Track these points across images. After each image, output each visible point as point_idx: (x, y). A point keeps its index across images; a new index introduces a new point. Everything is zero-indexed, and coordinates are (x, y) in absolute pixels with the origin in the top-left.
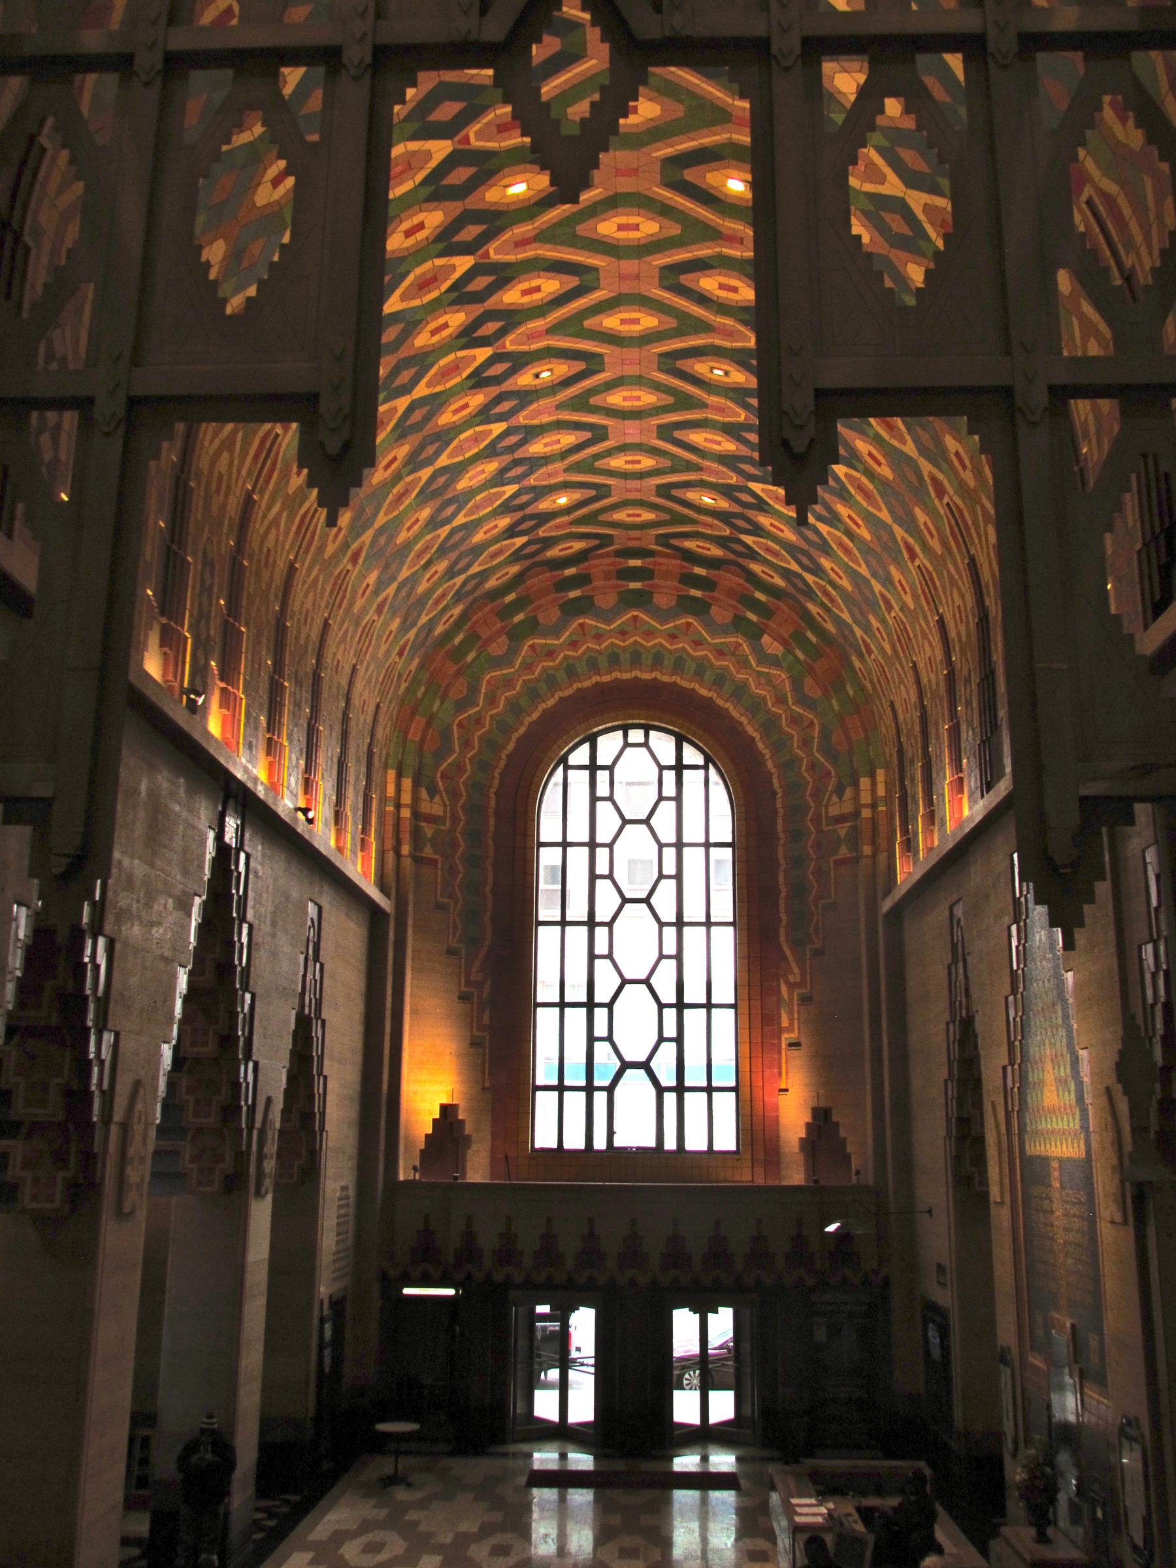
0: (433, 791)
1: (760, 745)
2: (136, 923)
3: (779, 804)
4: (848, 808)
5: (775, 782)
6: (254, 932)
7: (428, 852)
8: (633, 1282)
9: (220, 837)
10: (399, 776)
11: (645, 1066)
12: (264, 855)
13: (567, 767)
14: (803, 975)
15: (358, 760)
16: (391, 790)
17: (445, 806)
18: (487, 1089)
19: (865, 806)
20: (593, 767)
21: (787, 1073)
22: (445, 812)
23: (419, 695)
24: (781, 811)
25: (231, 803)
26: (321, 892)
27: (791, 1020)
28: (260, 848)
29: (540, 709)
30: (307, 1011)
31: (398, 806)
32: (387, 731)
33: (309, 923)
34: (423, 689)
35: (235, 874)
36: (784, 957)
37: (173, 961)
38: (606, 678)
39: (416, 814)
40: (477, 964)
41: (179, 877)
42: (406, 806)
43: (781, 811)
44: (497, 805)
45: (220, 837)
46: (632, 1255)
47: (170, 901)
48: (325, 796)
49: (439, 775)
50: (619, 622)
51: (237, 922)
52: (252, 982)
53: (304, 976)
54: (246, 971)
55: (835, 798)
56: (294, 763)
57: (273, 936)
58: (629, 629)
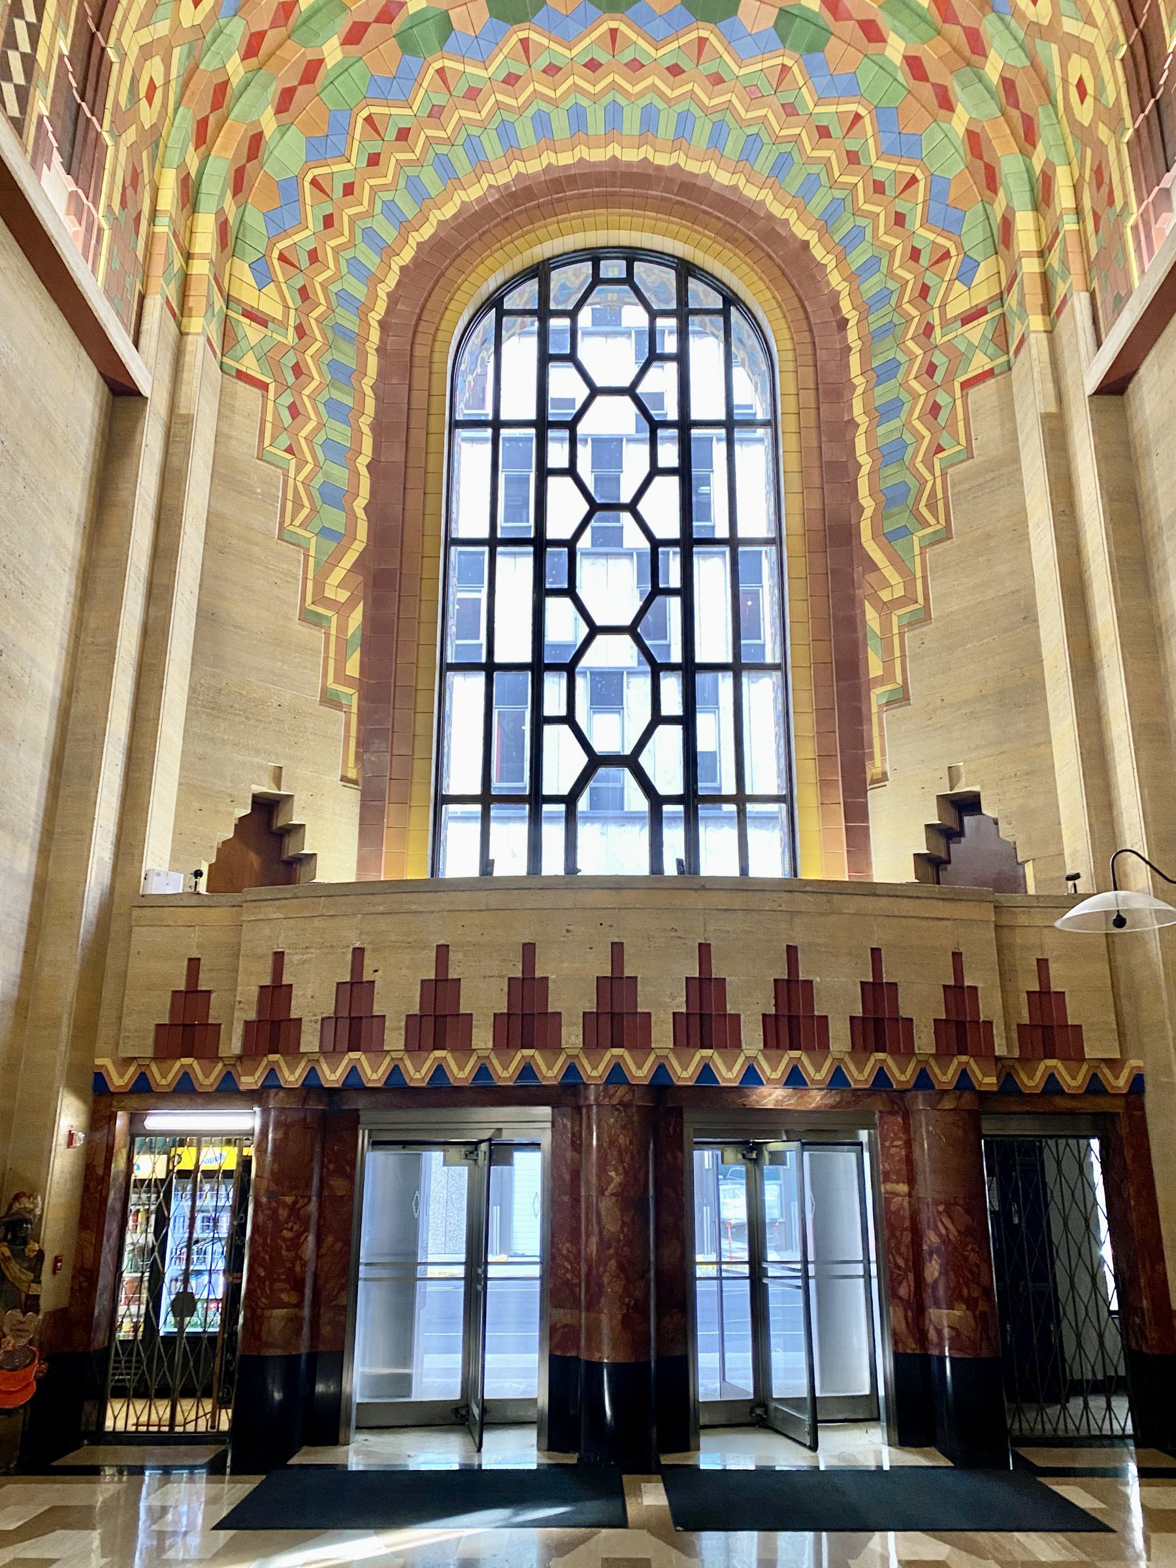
0: (263, 276)
1: (818, 252)
3: (852, 335)
4: (982, 293)
5: (846, 306)
8: (617, 1074)
11: (631, 761)
13: (501, 314)
14: (909, 584)
17: (286, 307)
18: (355, 782)
19: (1028, 254)
20: (543, 313)
21: (883, 753)
22: (286, 315)
24: (856, 345)
27: (888, 663)
36: (873, 567)
38: (566, 159)
40: (338, 575)
43: (856, 345)
46: (616, 1015)
50: (587, 41)
55: (958, 287)
58: (603, 57)
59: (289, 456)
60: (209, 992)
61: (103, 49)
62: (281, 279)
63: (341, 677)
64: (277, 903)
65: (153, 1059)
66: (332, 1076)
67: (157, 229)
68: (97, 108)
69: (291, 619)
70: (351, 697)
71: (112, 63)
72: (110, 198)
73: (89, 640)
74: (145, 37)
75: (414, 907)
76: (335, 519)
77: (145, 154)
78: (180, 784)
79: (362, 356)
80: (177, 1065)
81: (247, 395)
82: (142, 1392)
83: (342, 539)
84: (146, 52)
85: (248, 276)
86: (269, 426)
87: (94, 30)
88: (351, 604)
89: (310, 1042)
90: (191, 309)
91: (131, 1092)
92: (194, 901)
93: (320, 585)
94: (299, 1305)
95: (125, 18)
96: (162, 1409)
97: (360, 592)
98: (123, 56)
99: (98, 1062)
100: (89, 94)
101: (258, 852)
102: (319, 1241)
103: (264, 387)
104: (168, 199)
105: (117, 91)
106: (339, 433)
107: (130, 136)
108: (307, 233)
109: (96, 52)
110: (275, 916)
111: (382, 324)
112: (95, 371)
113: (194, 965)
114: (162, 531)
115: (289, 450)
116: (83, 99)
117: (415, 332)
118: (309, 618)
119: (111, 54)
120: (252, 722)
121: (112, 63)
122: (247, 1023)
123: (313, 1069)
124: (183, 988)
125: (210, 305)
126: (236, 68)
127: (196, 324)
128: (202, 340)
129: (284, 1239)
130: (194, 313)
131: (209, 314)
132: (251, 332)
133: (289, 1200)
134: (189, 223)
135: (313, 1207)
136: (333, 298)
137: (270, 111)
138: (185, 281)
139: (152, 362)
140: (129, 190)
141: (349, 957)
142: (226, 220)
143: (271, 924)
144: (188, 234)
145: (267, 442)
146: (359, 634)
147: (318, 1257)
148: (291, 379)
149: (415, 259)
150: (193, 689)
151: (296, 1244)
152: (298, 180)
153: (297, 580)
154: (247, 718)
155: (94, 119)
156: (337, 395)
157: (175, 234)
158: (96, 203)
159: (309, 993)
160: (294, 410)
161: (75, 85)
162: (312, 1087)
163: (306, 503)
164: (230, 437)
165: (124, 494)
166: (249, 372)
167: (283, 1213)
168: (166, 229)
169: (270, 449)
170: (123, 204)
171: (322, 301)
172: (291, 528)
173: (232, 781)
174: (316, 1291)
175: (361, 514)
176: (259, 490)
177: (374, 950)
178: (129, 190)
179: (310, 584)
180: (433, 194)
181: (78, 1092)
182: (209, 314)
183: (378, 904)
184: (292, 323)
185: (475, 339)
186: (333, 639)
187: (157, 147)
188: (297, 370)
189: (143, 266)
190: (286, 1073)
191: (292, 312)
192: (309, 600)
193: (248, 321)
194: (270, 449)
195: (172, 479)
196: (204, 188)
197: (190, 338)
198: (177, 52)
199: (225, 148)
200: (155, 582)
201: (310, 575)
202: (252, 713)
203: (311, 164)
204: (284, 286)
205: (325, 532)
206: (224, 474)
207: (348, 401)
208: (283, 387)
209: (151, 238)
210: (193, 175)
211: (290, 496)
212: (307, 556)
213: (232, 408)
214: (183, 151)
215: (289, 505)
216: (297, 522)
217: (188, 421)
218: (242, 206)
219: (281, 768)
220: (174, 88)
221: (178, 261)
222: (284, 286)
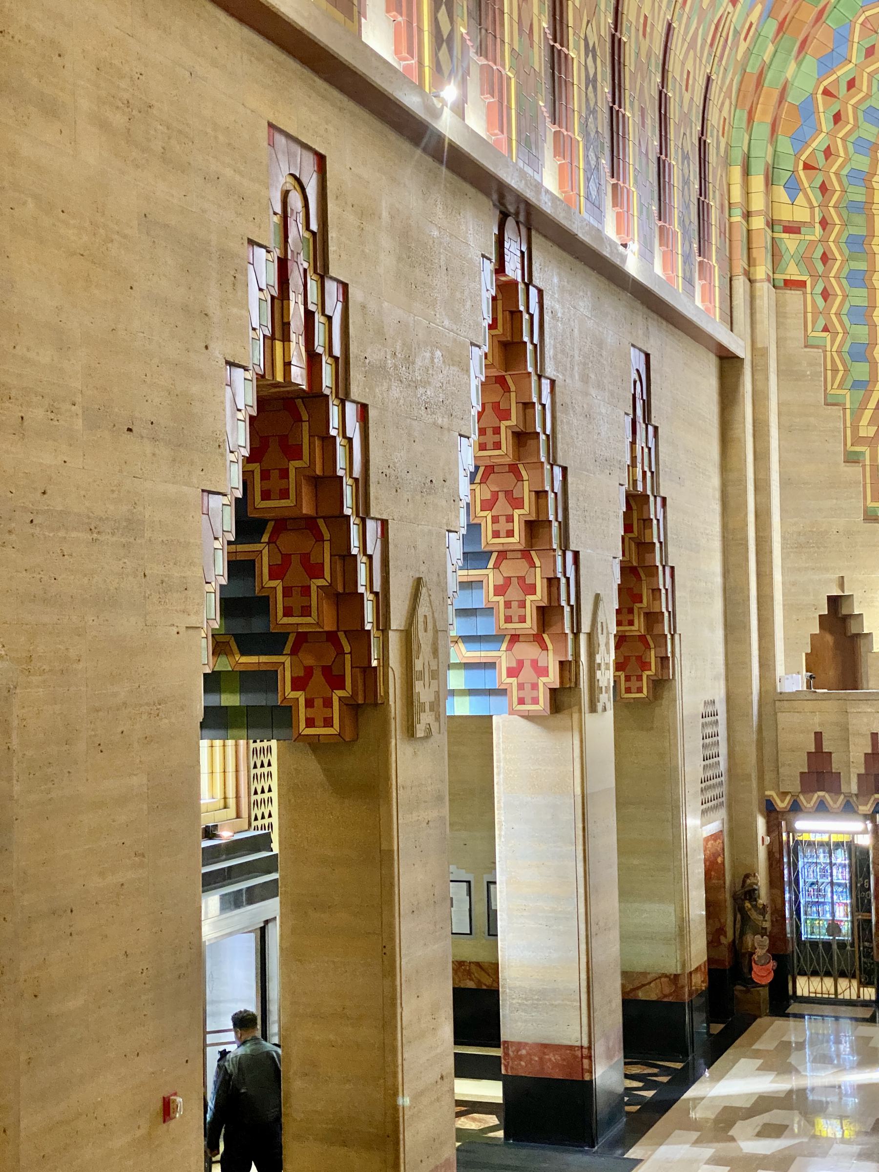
0: (793, 188)
2: (395, 384)
6: (557, 389)
7: (793, 272)
9: (500, 269)
10: (746, 172)
12: (562, 289)
15: (685, 157)
16: (737, 195)
17: (812, 208)
23: (767, 58)
25: (510, 223)
26: (647, 334)
28: (556, 280)
30: (640, 488)
31: (747, 215)
32: (725, 113)
33: (635, 376)
34: (771, 48)
35: (526, 316)
37: (449, 430)
39: (771, 224)
41: (447, 323)
42: (759, 213)
45: (500, 269)
47: (438, 353)
48: (641, 205)
51: (534, 378)
52: (560, 454)
53: (633, 443)
54: (552, 440)
56: (593, 163)
57: (586, 394)
59: (825, 334)
60: (830, 753)
67: (733, 219)
78: (784, 605)
80: (816, 796)
81: (793, 296)
86: (809, 315)
90: (755, 259)
91: (789, 811)
93: (855, 428)
99: (768, 793)
103: (803, 284)
108: (823, 135)
110: (869, 710)
113: (818, 736)
115: (826, 329)
118: (852, 459)
120: (822, 549)
124: (813, 750)
132: (790, 243)
148: (820, 267)
152: (813, 96)
153: (839, 432)
154: (818, 548)
160: (826, 295)
163: (841, 367)
171: (838, 188)
176: (808, 373)
184: (817, 220)
186: (868, 468)
191: (817, 209)
201: (848, 424)
204: (809, 190)
205: (857, 385)
207: (863, 266)
211: (829, 367)
215: (829, 373)
216: (835, 386)
219: (842, 577)
222: (809, 190)
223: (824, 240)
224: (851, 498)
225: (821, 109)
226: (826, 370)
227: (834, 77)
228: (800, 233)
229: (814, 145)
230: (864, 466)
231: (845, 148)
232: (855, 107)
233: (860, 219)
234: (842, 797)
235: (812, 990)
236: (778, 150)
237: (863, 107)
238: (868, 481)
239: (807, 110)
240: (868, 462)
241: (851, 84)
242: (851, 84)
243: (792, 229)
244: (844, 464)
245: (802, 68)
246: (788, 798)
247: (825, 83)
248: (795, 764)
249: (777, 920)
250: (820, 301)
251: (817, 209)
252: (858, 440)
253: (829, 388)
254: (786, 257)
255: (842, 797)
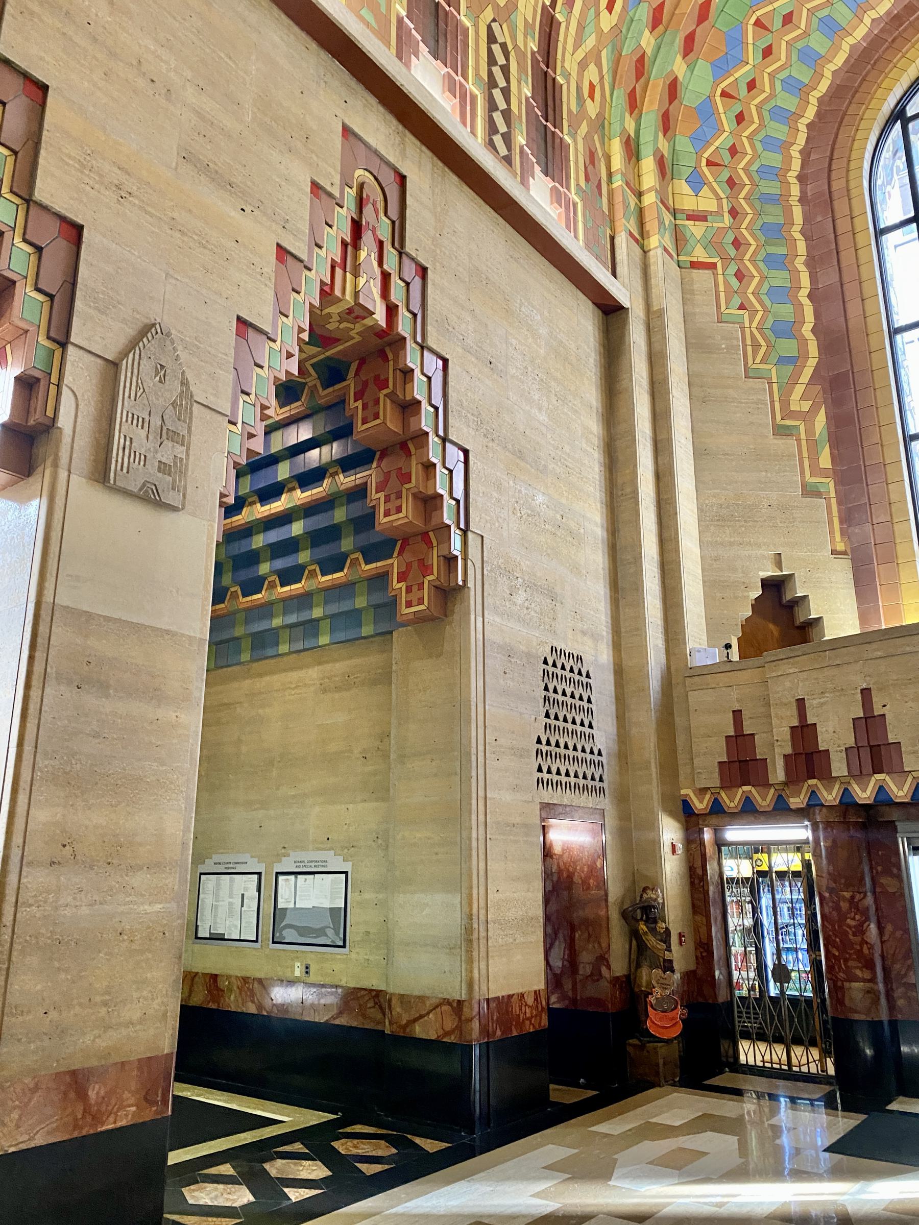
0: (697, 183)
7: (700, 254)
17: (719, 199)
22: (720, 206)
29: (846, 47)
40: (799, 390)
44: (803, 192)
49: (704, 162)
60: (753, 734)
61: (554, 79)
62: (711, 179)
63: (817, 471)
64: (791, 660)
65: (721, 788)
66: (864, 794)
67: (614, 186)
68: (557, 124)
69: (767, 437)
70: (829, 485)
71: (561, 85)
72: (577, 179)
73: (620, 493)
74: (580, 54)
75: (908, 649)
76: (788, 347)
77: (596, 137)
78: (704, 582)
79: (788, 210)
80: (740, 791)
82: (761, 1037)
83: (796, 361)
84: (583, 65)
85: (686, 189)
86: (722, 295)
87: (545, 69)
88: (814, 410)
89: (839, 767)
90: (648, 232)
92: (728, 667)
93: (785, 404)
94: (873, 980)
95: (564, 48)
96: (779, 1050)
97: (820, 399)
98: (568, 77)
99: (683, 792)
100: (551, 117)
101: (775, 623)
102: (881, 929)
103: (713, 266)
104: (617, 162)
105: (569, 103)
106: (779, 278)
107: (584, 129)
108: (725, 135)
109: (550, 82)
110: (791, 671)
111: (801, 178)
112: (590, 303)
113: (737, 714)
114: (657, 400)
115: (742, 307)
116: (547, 121)
117: (830, 171)
118: (781, 431)
119: (560, 80)
121: (561, 85)
122: (786, 756)
123: (846, 789)
124: (732, 734)
125: (661, 223)
126: (647, 41)
127: (654, 241)
128: (660, 251)
129: (850, 927)
130: (651, 233)
131: (662, 230)
132: (696, 230)
133: (847, 895)
134: (636, 170)
135: (869, 900)
136: (754, 175)
137: (679, 58)
138: (641, 212)
139: (627, 281)
140: (590, 168)
141: (859, 697)
142: (662, 156)
143: (790, 678)
144: (636, 177)
145: (723, 307)
146: (825, 433)
147: (882, 942)
148: (732, 252)
149: (818, 114)
150: (700, 510)
151: (860, 930)
152: (710, 98)
154: (745, 521)
155: (557, 130)
156: (772, 250)
157: (627, 184)
158: (568, 188)
159: (831, 730)
160: (739, 275)
161: (540, 114)
162: (848, 805)
163: (763, 343)
164: (694, 314)
165: (624, 384)
166: (700, 260)
167: (844, 906)
168: (620, 183)
169: (727, 311)
170: (587, 179)
172: (754, 366)
173: (743, 572)
174: (886, 971)
175: (809, 336)
177: (880, 689)
178: (590, 168)
179: (777, 405)
180: (822, 52)
181: (672, 814)
182: (662, 230)
183: (875, 650)
184: (726, 209)
185: (886, 154)
186: (804, 443)
187: (604, 128)
188: (736, 243)
189: (609, 216)
190: (825, 794)
191: (725, 201)
192: (778, 417)
193: (692, 222)
194: (727, 311)
195: (656, 361)
196: (642, 141)
197: (651, 253)
198: (604, 54)
199: (651, 102)
200: (658, 438)
201: (776, 398)
202: (749, 517)
203: (717, 82)
204: (714, 184)
206: (696, 344)
207: (783, 251)
208: (727, 260)
209: (611, 193)
210: (632, 135)
211: (749, 342)
212: (770, 384)
213: (692, 292)
214: (622, 120)
215: (749, 349)
216: (758, 360)
217: (661, 313)
218: (672, 140)
220: (607, 79)
221: (632, 200)
222: (714, 184)
223: (735, 227)
224: (786, 471)
225: (721, 110)
226: (745, 345)
227: (731, 79)
228: (706, 221)
229: (717, 144)
230: (799, 440)
231: (753, 146)
232: (759, 108)
233: (777, 210)
234: (772, 791)
235: (767, 1058)
236: (677, 148)
237: (768, 106)
238: (805, 455)
239: (706, 111)
240: (803, 436)
241: (751, 85)
242: (751, 85)
243: (698, 217)
244: (772, 437)
245: (695, 72)
246: (708, 796)
247: (723, 85)
248: (709, 752)
249: (703, 957)
250: (734, 283)
251: (725, 201)
252: (788, 414)
253: (750, 362)
254: (692, 241)
255: (772, 791)
